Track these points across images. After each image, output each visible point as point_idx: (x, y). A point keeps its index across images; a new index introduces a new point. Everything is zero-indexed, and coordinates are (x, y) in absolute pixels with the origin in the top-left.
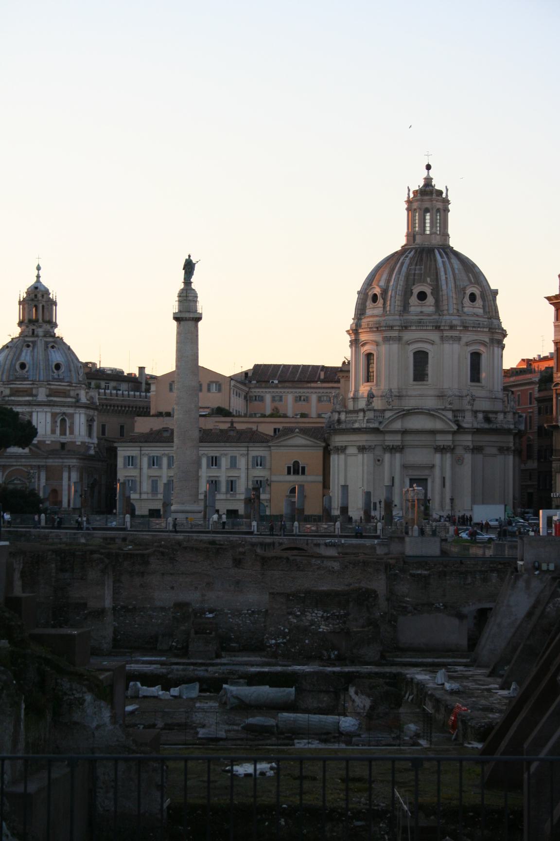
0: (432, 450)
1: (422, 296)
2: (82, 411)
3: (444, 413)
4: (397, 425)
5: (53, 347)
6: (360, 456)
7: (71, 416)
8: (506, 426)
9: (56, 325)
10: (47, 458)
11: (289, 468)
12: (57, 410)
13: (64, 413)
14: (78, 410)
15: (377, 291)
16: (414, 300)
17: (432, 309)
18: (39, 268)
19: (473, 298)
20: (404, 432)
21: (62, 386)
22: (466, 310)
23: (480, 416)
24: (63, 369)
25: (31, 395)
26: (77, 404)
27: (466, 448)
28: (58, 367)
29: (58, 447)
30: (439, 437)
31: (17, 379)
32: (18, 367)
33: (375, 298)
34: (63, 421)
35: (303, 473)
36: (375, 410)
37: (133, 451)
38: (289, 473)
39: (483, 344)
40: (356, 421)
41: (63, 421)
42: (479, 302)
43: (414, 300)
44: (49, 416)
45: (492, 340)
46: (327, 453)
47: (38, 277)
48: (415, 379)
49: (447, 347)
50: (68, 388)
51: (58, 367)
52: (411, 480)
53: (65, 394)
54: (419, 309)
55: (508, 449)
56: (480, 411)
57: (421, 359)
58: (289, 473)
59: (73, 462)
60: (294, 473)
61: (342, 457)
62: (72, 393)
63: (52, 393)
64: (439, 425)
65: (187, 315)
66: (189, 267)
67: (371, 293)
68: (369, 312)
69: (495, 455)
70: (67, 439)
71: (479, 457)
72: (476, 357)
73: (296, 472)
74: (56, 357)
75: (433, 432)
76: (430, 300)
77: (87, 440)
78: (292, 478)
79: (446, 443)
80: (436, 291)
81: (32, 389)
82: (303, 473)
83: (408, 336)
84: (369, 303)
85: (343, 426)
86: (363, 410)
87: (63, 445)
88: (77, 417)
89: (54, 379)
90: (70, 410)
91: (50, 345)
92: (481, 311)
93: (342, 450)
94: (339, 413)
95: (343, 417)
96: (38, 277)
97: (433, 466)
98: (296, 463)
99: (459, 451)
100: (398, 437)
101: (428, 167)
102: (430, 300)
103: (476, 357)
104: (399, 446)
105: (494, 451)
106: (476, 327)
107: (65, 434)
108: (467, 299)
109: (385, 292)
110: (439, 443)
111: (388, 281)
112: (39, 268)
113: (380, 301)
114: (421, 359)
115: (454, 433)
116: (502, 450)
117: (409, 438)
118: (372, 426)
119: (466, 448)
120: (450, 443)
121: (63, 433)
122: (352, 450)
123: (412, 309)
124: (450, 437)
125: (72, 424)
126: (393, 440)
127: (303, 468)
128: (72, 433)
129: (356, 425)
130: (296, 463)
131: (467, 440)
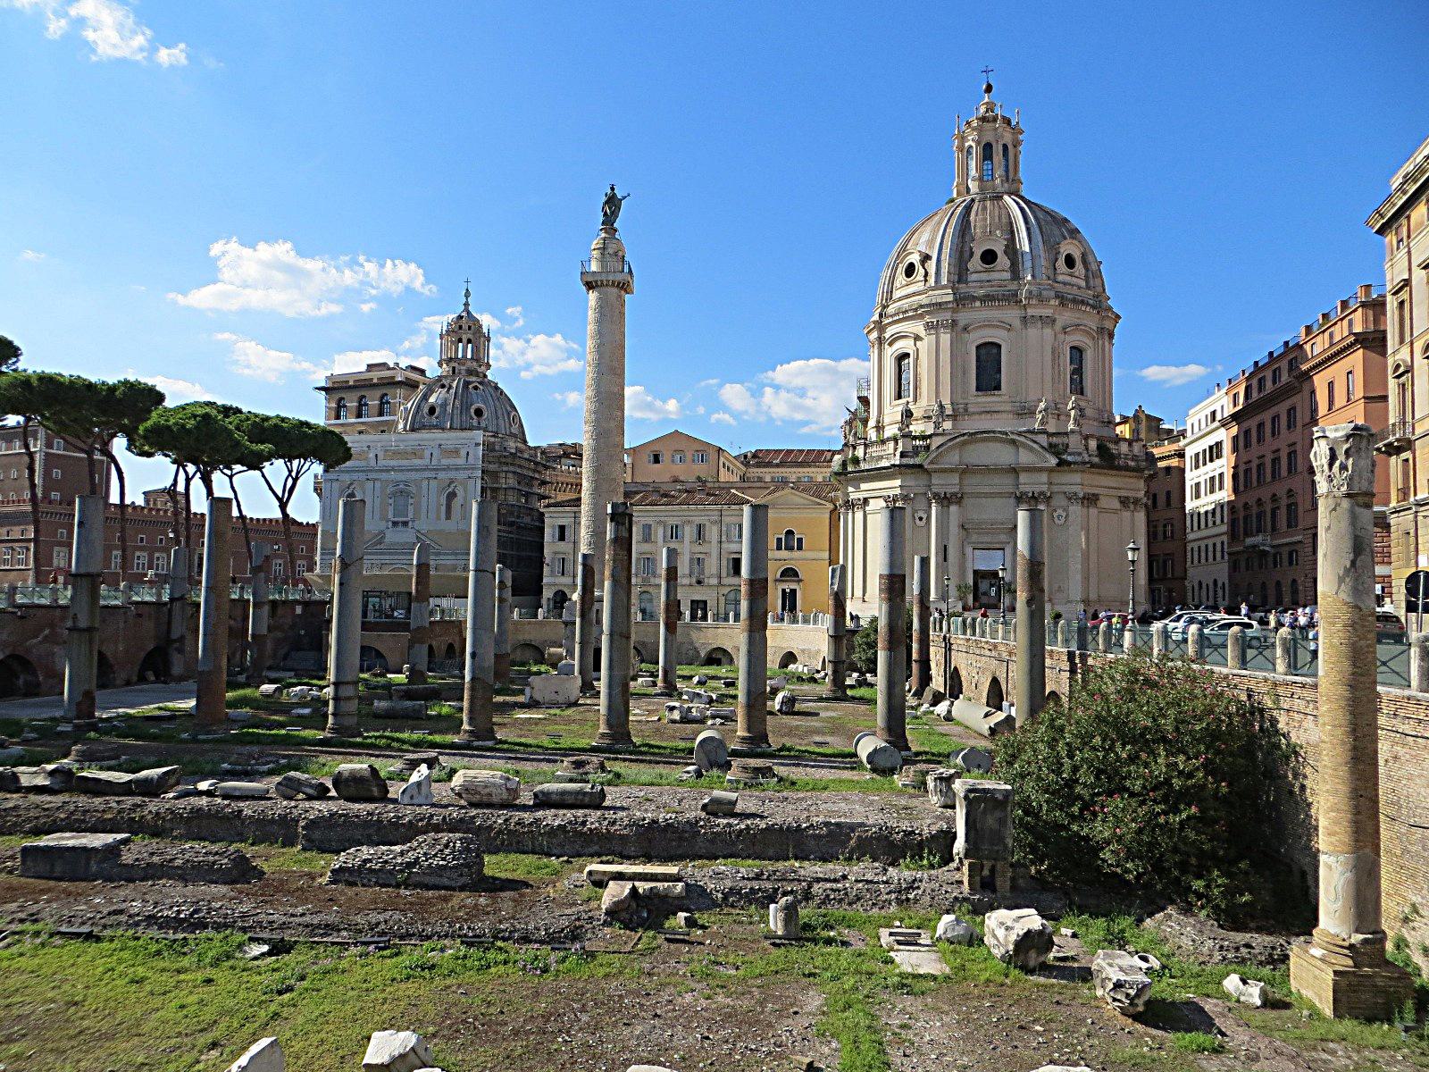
0: (1012, 501)
3: (1033, 437)
4: (953, 459)
9: (488, 366)
15: (915, 258)
16: (975, 263)
17: (1007, 275)
18: (467, 294)
19: (1070, 261)
20: (966, 471)
22: (1060, 278)
23: (1093, 444)
27: (1071, 497)
28: (479, 412)
30: (1023, 478)
32: (426, 410)
35: (800, 548)
36: (915, 438)
40: (881, 458)
43: (975, 263)
45: (1101, 330)
47: (466, 304)
48: (978, 389)
49: (1033, 332)
50: (492, 439)
55: (1136, 501)
56: (1092, 436)
57: (989, 357)
64: (1025, 458)
65: (604, 277)
69: (1115, 511)
71: (1093, 511)
75: (1014, 471)
76: (1003, 261)
79: (1037, 489)
83: (964, 317)
84: (901, 278)
86: (895, 440)
92: (1083, 284)
94: (854, 448)
95: (860, 452)
96: (466, 304)
99: (1059, 501)
102: (1003, 261)
103: (1077, 352)
104: (954, 494)
105: (1117, 505)
108: (1061, 263)
109: (926, 258)
110: (1023, 488)
112: (467, 294)
114: (989, 357)
115: (1050, 470)
117: (974, 484)
118: (905, 461)
119: (1071, 497)
120: (1044, 488)
124: (1044, 477)
126: (950, 484)
127: (800, 540)
129: (885, 463)
131: (1075, 482)
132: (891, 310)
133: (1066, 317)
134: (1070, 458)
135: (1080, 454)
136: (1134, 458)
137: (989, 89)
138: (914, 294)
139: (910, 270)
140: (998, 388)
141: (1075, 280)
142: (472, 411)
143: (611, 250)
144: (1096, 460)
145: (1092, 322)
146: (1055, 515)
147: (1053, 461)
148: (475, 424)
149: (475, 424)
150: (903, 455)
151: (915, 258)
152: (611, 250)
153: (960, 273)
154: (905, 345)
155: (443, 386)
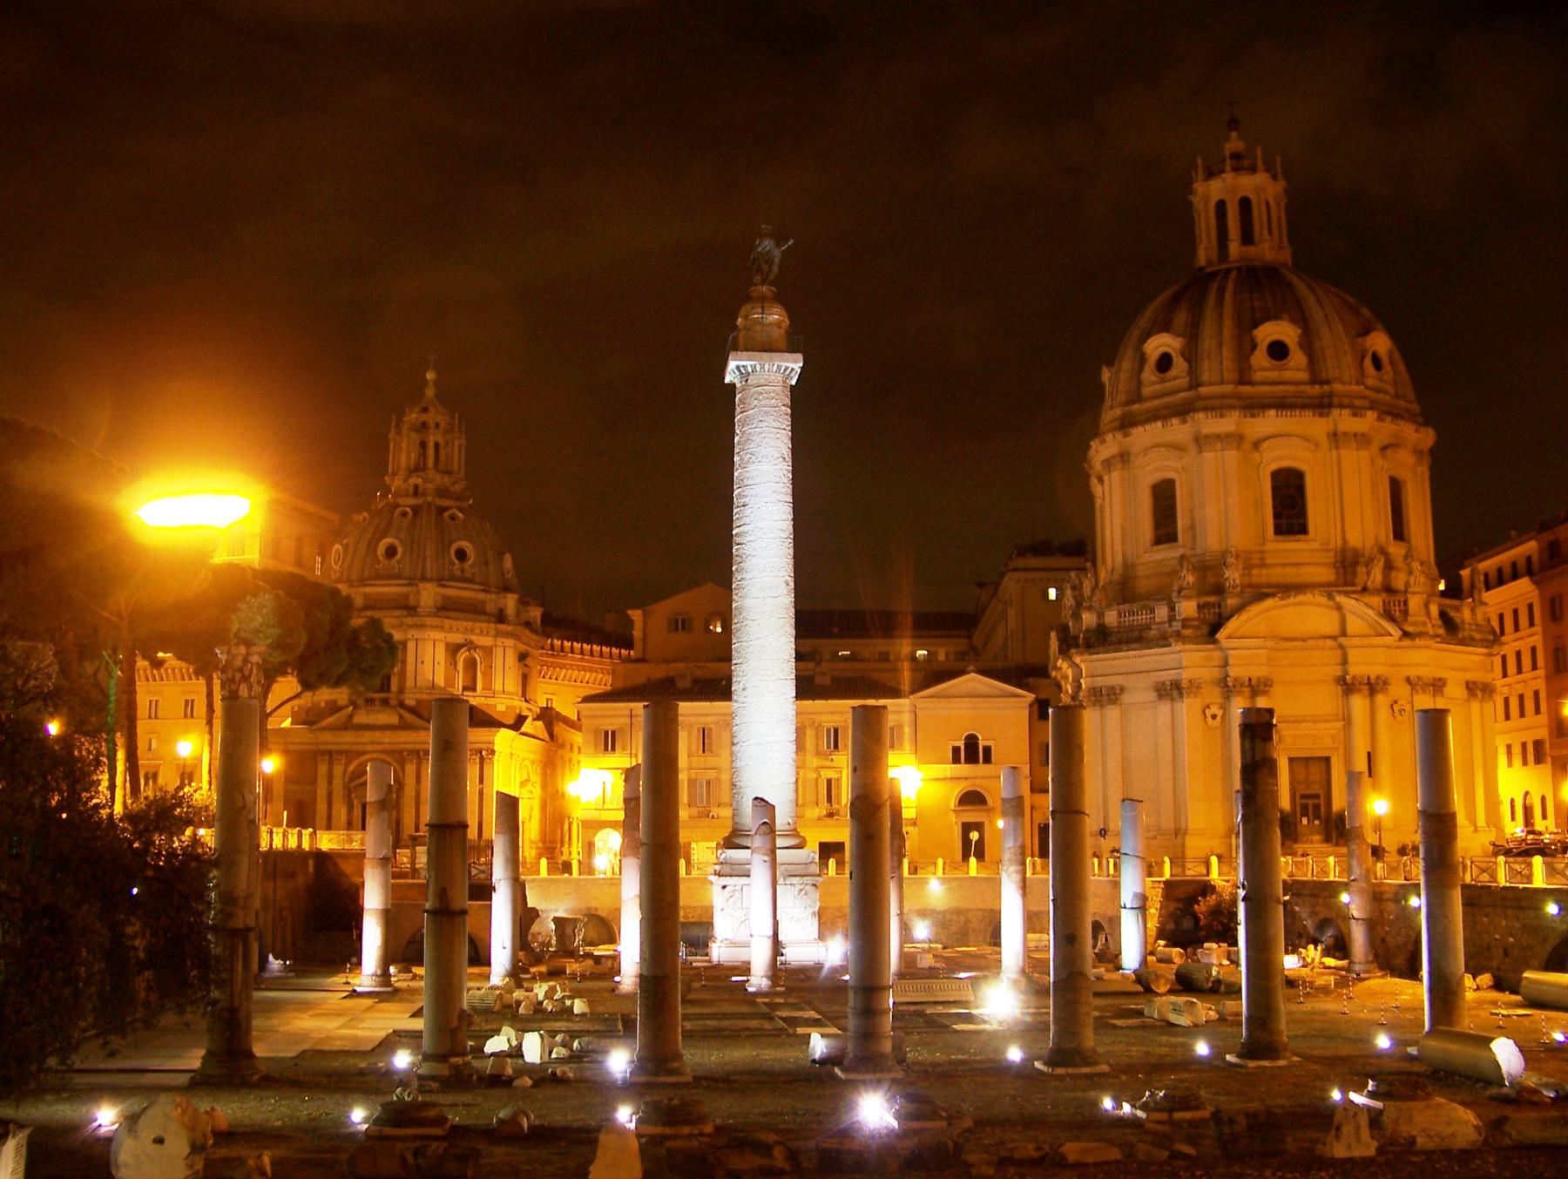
1: (1278, 351)
6: (1164, 708)
7: (488, 651)
11: (956, 750)
14: (500, 641)
16: (1260, 358)
31: (379, 576)
35: (987, 760)
38: (956, 760)
41: (471, 665)
43: (1260, 358)
48: (1279, 531)
50: (481, 596)
52: (1291, 760)
58: (956, 760)
60: (967, 762)
61: (1113, 713)
73: (972, 758)
81: (407, 596)
82: (987, 760)
88: (499, 653)
89: (453, 578)
91: (446, 514)
92: (1391, 389)
93: (1107, 696)
98: (971, 742)
102: (1297, 358)
107: (474, 689)
108: (1368, 362)
113: (1179, 366)
122: (1139, 693)
127: (987, 750)
128: (488, 686)
130: (971, 742)
134: (1410, 629)
135: (1424, 624)
140: (1303, 530)
141: (1383, 386)
142: (452, 552)
146: (1396, 708)
148: (458, 573)
149: (458, 573)
154: (1151, 470)
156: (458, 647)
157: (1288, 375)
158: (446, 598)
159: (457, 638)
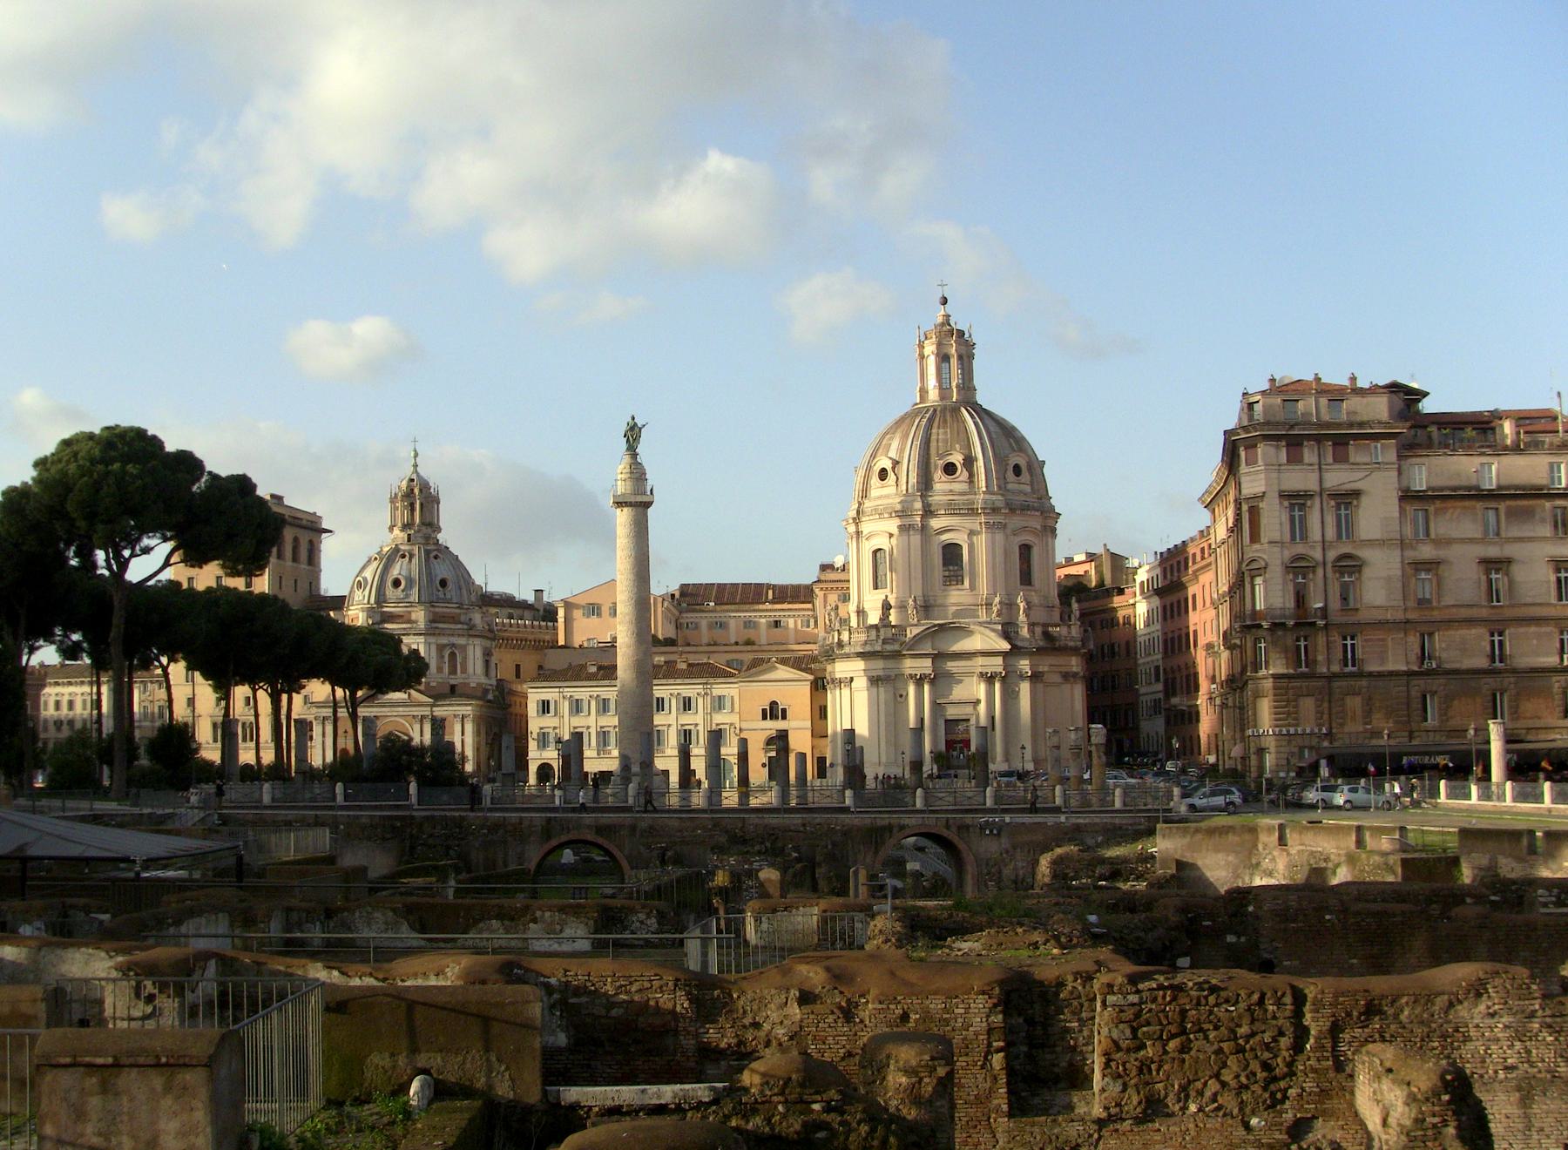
2: (477, 641)
5: (436, 557)
7: (464, 648)
8: (1071, 644)
9: (439, 530)
10: (433, 705)
11: (764, 711)
12: (444, 640)
13: (453, 645)
15: (888, 465)
17: (964, 487)
18: (416, 455)
19: (1017, 470)
21: (451, 610)
22: (1010, 486)
23: (1038, 630)
24: (450, 585)
25: (410, 621)
26: (470, 631)
28: (443, 583)
29: (447, 690)
32: (389, 583)
33: (883, 474)
34: (453, 655)
35: (784, 717)
37: (550, 694)
38: (764, 718)
39: (1033, 532)
41: (453, 655)
42: (1025, 477)
43: (938, 475)
44: (433, 648)
45: (1045, 527)
46: (820, 686)
47: (416, 466)
51: (443, 583)
53: (453, 619)
54: (947, 487)
55: (1075, 675)
58: (764, 718)
59: (467, 710)
61: (846, 692)
62: (463, 618)
63: (434, 619)
66: (633, 434)
67: (877, 468)
68: (874, 493)
69: (1058, 685)
70: (457, 680)
71: (1040, 686)
72: (1026, 550)
73: (774, 717)
74: (442, 571)
76: (962, 474)
77: (483, 680)
78: (769, 724)
80: (969, 461)
84: (875, 480)
85: (847, 650)
87: (453, 687)
90: (461, 641)
92: (1028, 488)
96: (416, 466)
97: (979, 701)
98: (774, 704)
100: (928, 662)
101: (944, 301)
102: (962, 474)
103: (1026, 550)
105: (1057, 678)
106: (1025, 508)
108: (1010, 475)
109: (896, 463)
111: (901, 450)
112: (416, 455)
113: (891, 477)
115: (1005, 654)
116: (1067, 677)
118: (889, 647)
120: (1000, 669)
121: (453, 671)
123: (937, 486)
124: (999, 660)
125: (465, 659)
127: (784, 711)
128: (464, 671)
130: (774, 704)
131: (1024, 665)
132: (868, 504)
133: (1016, 521)
136: (1072, 639)
137: (944, 301)
138: (887, 496)
139: (883, 474)
143: (638, 474)
144: (1041, 643)
145: (1035, 523)
147: (1006, 646)
150: (885, 642)
151: (888, 465)
152: (638, 474)
153: (925, 483)
155: (403, 556)
156: (444, 646)
157: (957, 487)
158: (435, 614)
159: (444, 640)
